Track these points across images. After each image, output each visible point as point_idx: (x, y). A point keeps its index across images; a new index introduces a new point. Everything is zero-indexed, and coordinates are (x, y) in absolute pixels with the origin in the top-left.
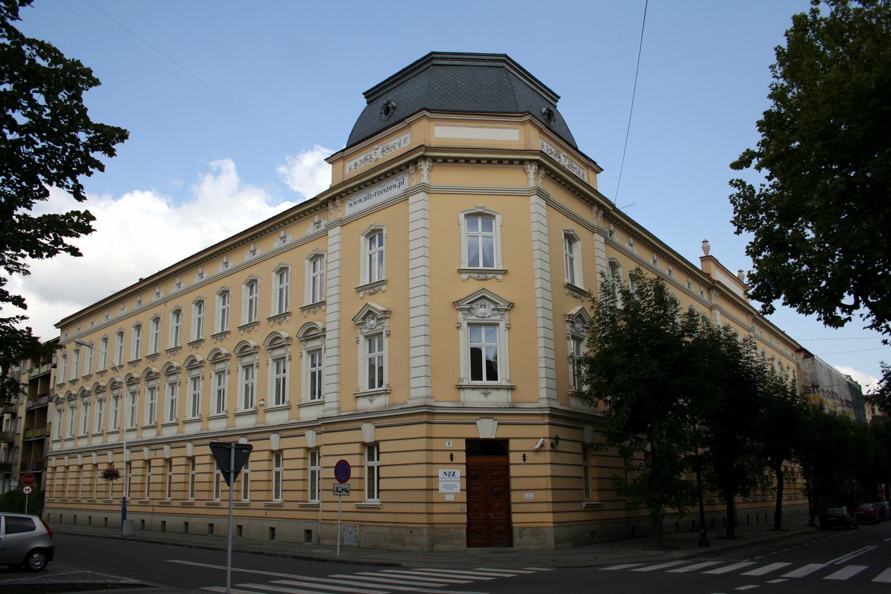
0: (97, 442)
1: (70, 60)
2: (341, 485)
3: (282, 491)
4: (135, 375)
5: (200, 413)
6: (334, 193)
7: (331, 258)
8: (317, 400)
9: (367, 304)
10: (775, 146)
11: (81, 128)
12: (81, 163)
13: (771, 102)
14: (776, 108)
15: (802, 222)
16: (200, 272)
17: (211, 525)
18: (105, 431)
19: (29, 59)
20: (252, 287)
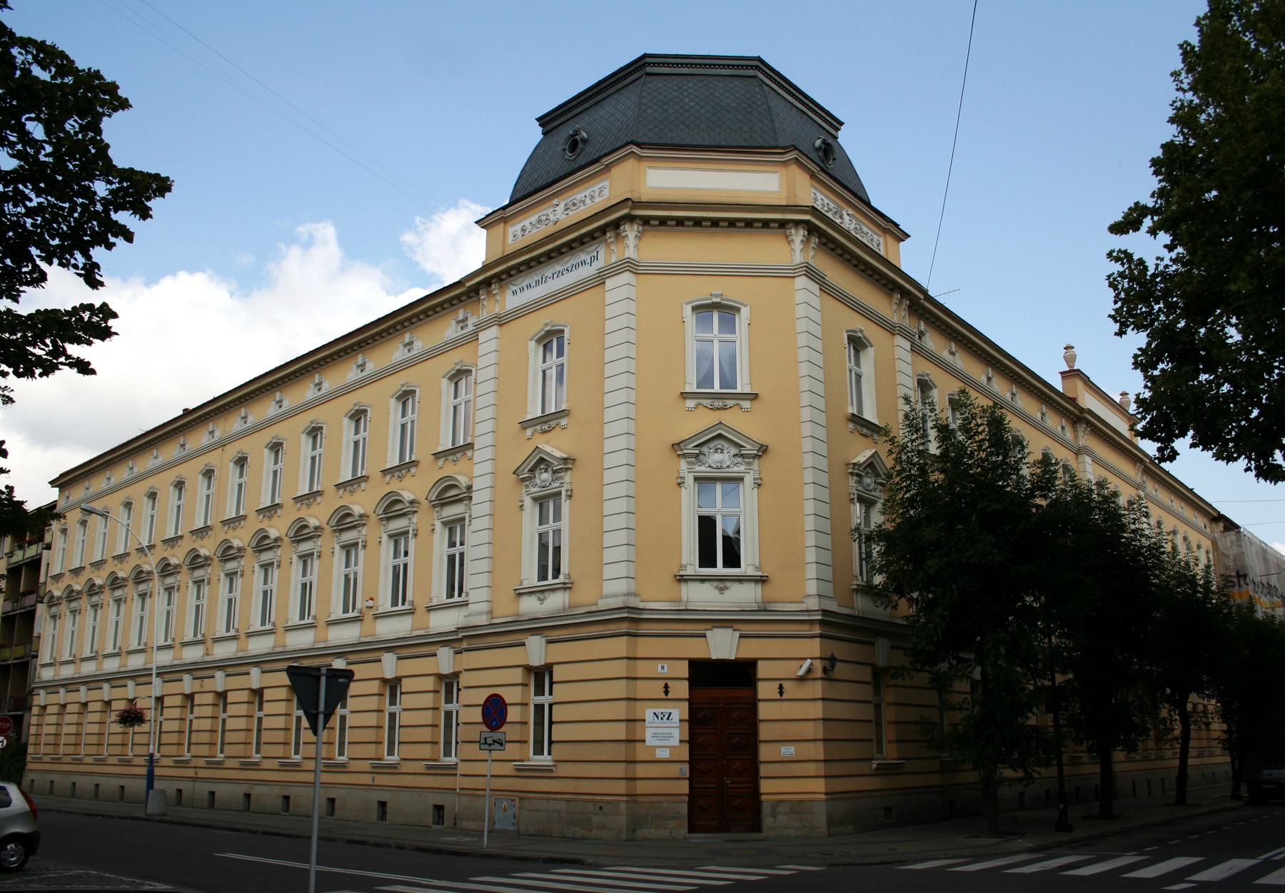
0: (111, 666)
1: (84, 70)
2: (492, 734)
3: (400, 743)
4: (174, 561)
5: (273, 619)
6: (489, 274)
7: (482, 375)
8: (456, 598)
9: (537, 447)
10: (1180, 197)
11: (99, 176)
12: (97, 229)
13: (1174, 129)
14: (1181, 138)
15: (1221, 316)
16: (278, 399)
17: (287, 798)
18: (124, 650)
19: (21, 69)
20: (358, 421)
